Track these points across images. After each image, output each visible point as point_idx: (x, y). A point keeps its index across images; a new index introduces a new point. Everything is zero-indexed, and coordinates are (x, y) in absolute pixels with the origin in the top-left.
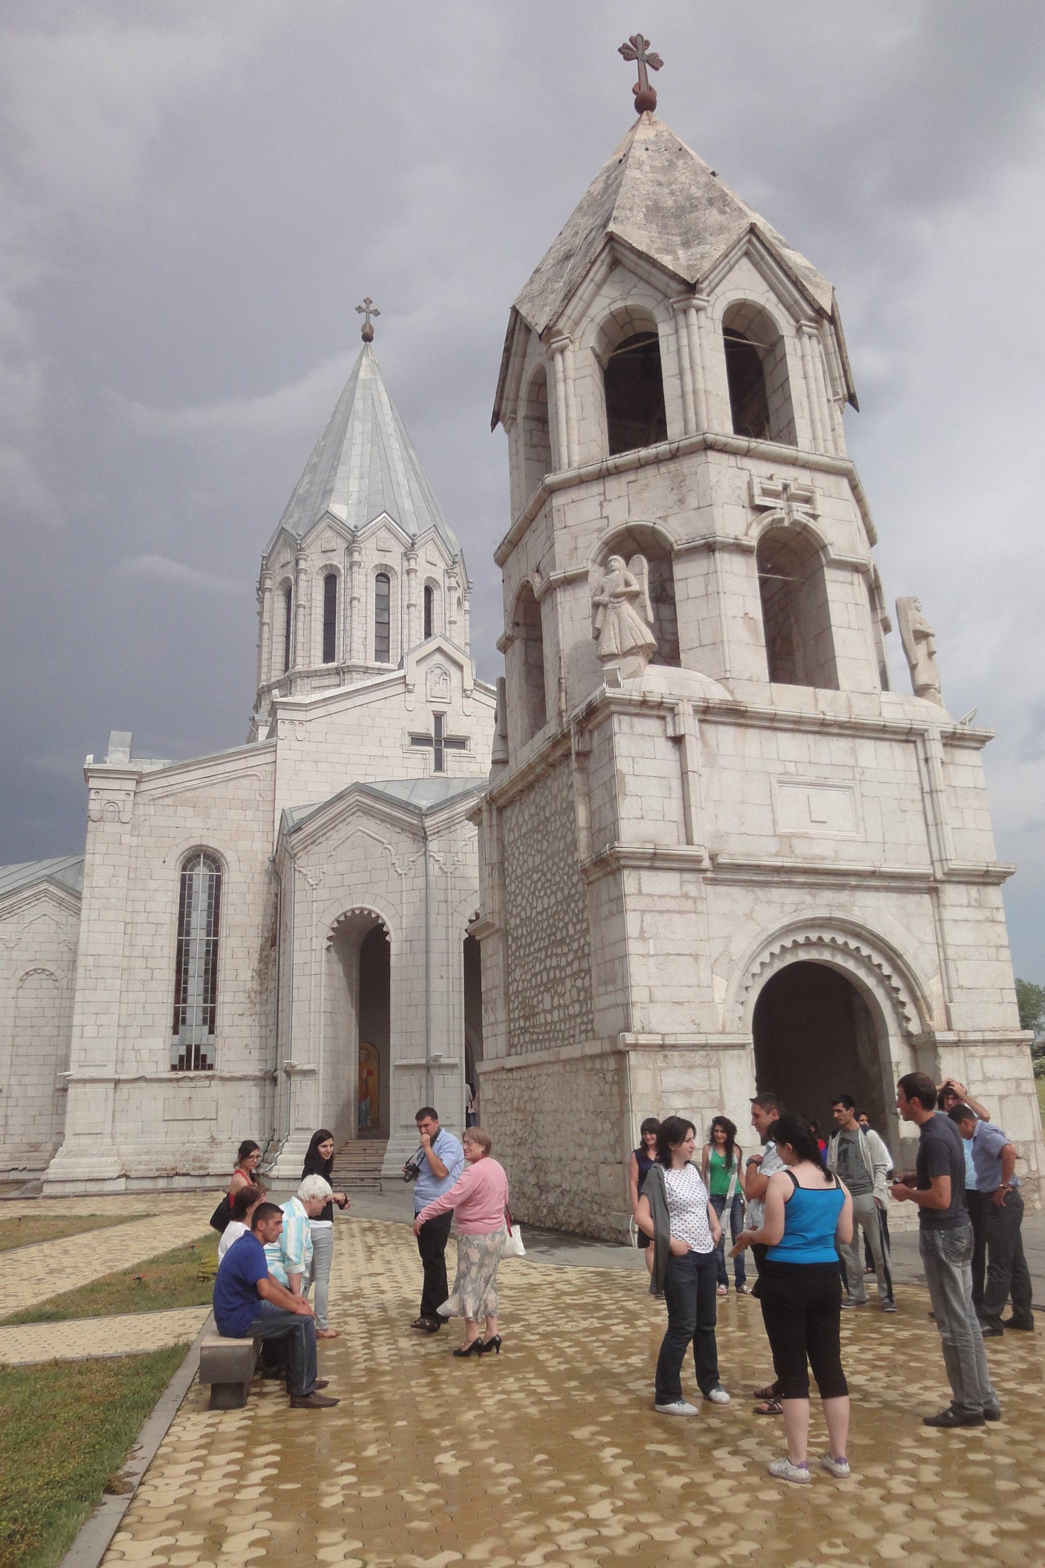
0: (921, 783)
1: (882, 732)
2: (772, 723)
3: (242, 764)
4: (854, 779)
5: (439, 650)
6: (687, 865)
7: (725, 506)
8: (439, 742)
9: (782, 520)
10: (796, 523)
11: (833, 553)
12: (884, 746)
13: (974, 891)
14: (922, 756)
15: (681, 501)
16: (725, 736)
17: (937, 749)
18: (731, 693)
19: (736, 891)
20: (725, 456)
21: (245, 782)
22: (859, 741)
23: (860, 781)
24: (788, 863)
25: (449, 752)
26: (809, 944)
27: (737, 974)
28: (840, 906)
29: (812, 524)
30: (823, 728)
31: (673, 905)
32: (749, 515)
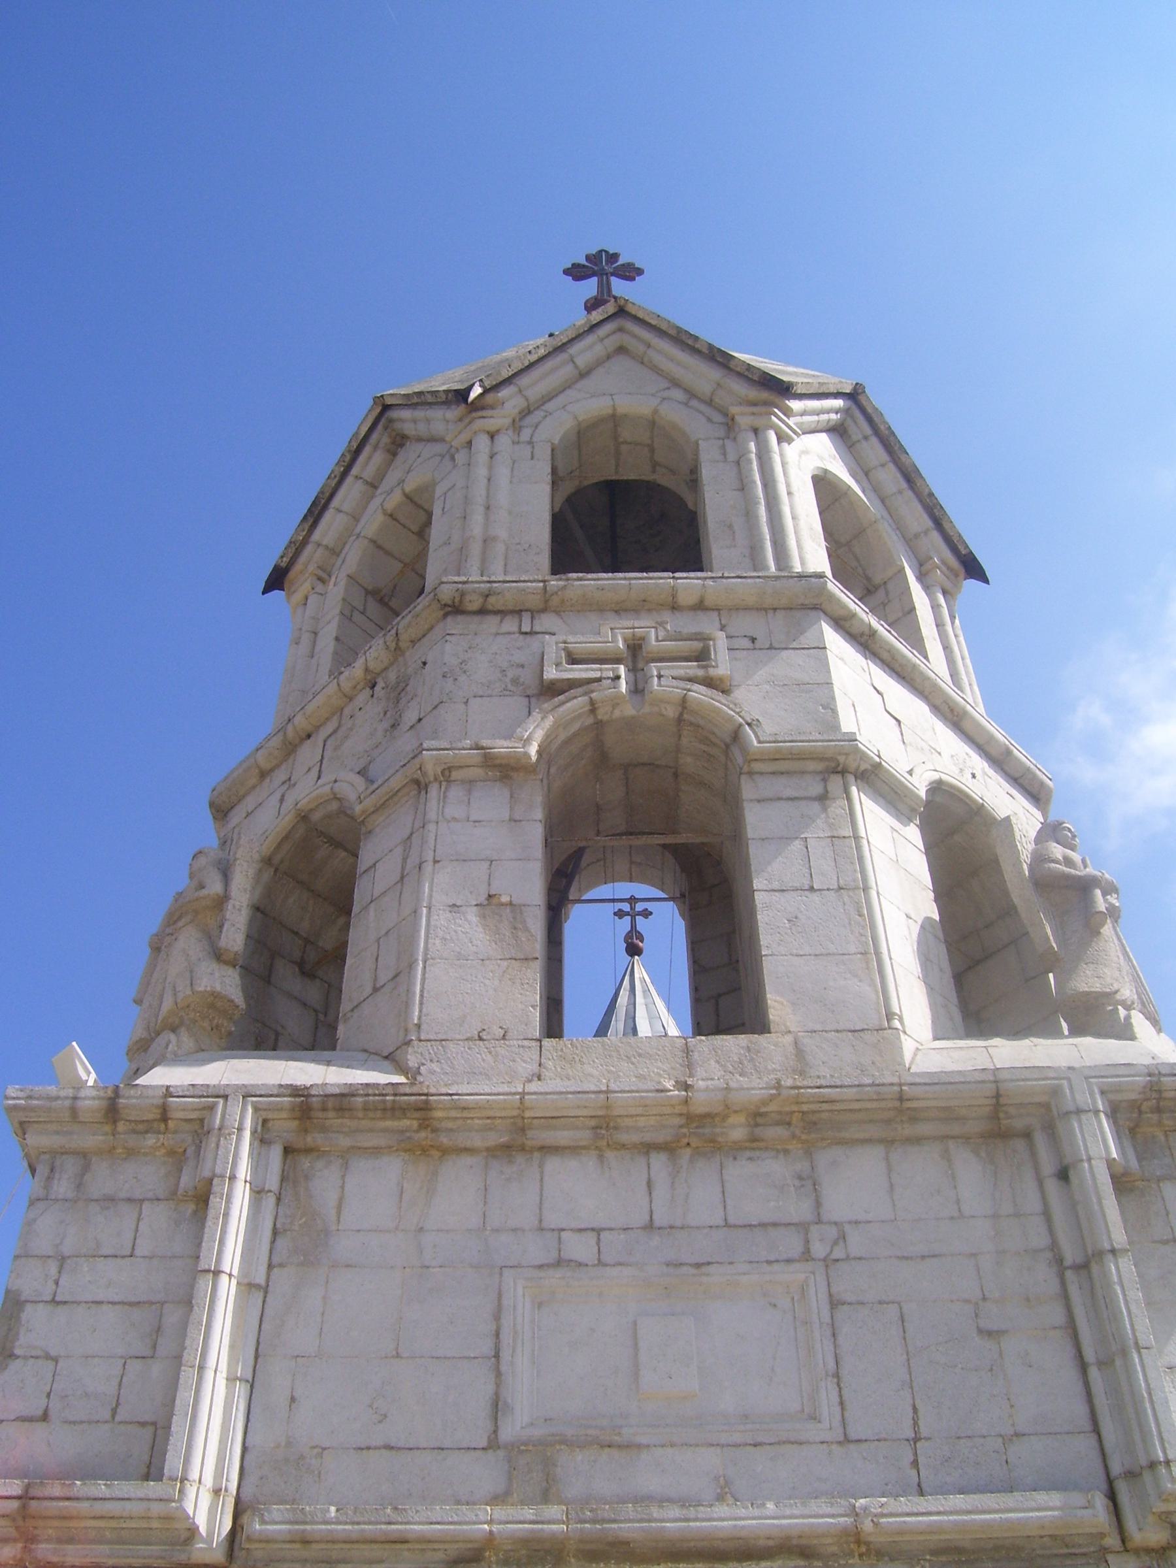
0: (1054, 1246)
4: (807, 1255)
7: (474, 703)
14: (1048, 1167)
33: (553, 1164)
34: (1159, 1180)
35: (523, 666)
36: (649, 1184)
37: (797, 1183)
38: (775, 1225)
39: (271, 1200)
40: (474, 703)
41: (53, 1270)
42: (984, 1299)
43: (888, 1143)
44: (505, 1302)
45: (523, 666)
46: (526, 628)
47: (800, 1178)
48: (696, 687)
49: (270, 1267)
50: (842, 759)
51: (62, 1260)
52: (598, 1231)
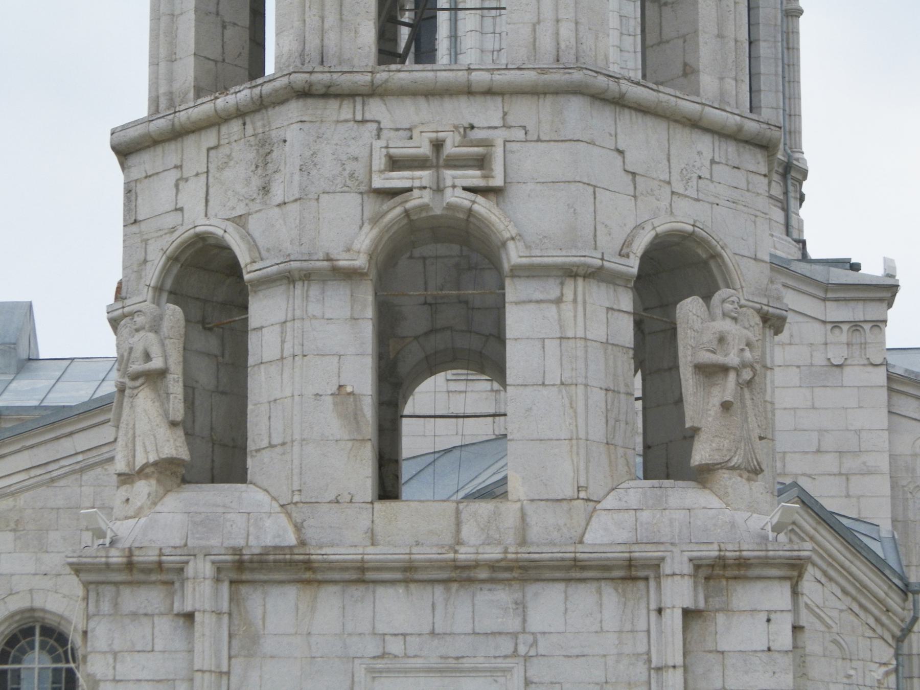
0: (648, 653)
1: (575, 571)
2: (361, 575)
7: (324, 198)
9: (424, 207)
10: (450, 207)
11: (514, 255)
12: (584, 597)
14: (653, 606)
15: (265, 190)
17: (679, 593)
18: (298, 528)
20: (333, 104)
22: (532, 589)
23: (527, 658)
29: (482, 206)
30: (460, 575)
32: (372, 205)
33: (381, 591)
34: (717, 611)
35: (356, 159)
36: (433, 605)
37: (514, 607)
38: (500, 633)
39: (225, 619)
40: (324, 198)
41: (111, 661)
42: (606, 682)
43: (569, 580)
44: (356, 679)
45: (356, 159)
46: (359, 117)
47: (516, 603)
48: (480, 199)
49: (230, 658)
50: (575, 269)
51: (115, 654)
52: (404, 635)
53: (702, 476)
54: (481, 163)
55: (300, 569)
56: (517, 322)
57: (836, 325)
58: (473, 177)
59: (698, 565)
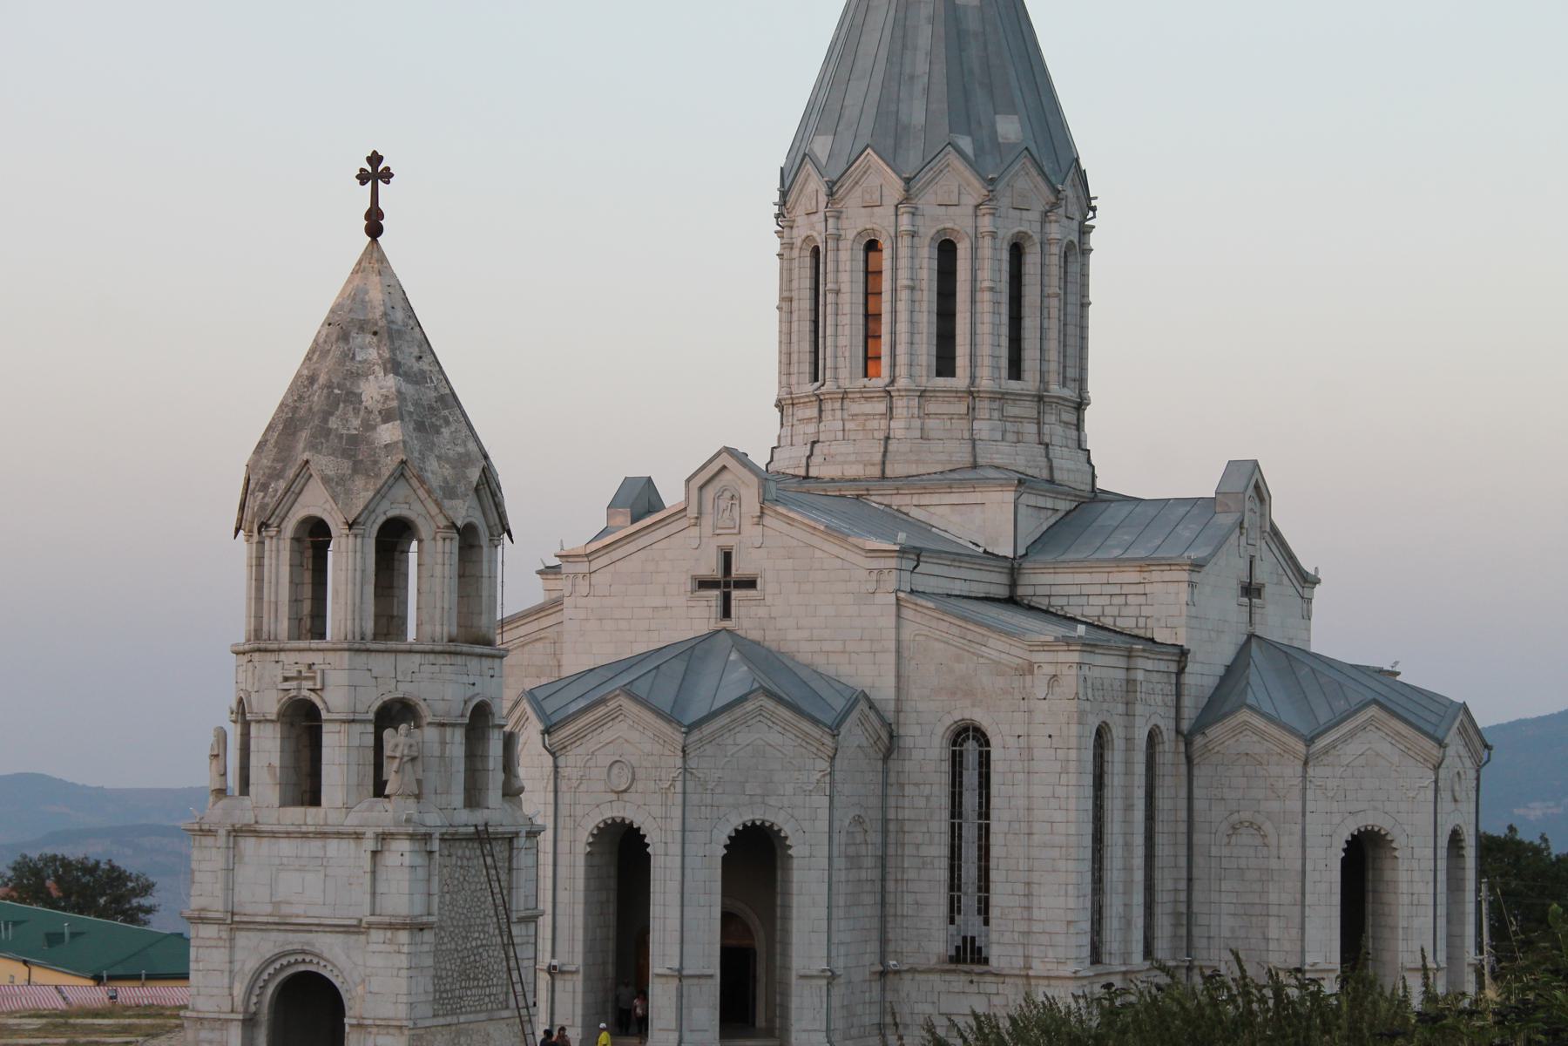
1: (339, 835)
2: (274, 835)
3: (534, 626)
5: (724, 467)
6: (219, 922)
8: (727, 585)
11: (324, 715)
13: (389, 934)
16: (248, 844)
17: (369, 845)
19: (251, 934)
21: (539, 645)
24: (271, 920)
25: (735, 594)
26: (296, 962)
27: (246, 982)
28: (308, 944)
29: (314, 697)
31: (213, 943)
32: (281, 694)
53: (388, 797)
54: (313, 678)
55: (254, 832)
56: (327, 739)
57: (871, 571)
58: (309, 684)
59: (377, 835)
